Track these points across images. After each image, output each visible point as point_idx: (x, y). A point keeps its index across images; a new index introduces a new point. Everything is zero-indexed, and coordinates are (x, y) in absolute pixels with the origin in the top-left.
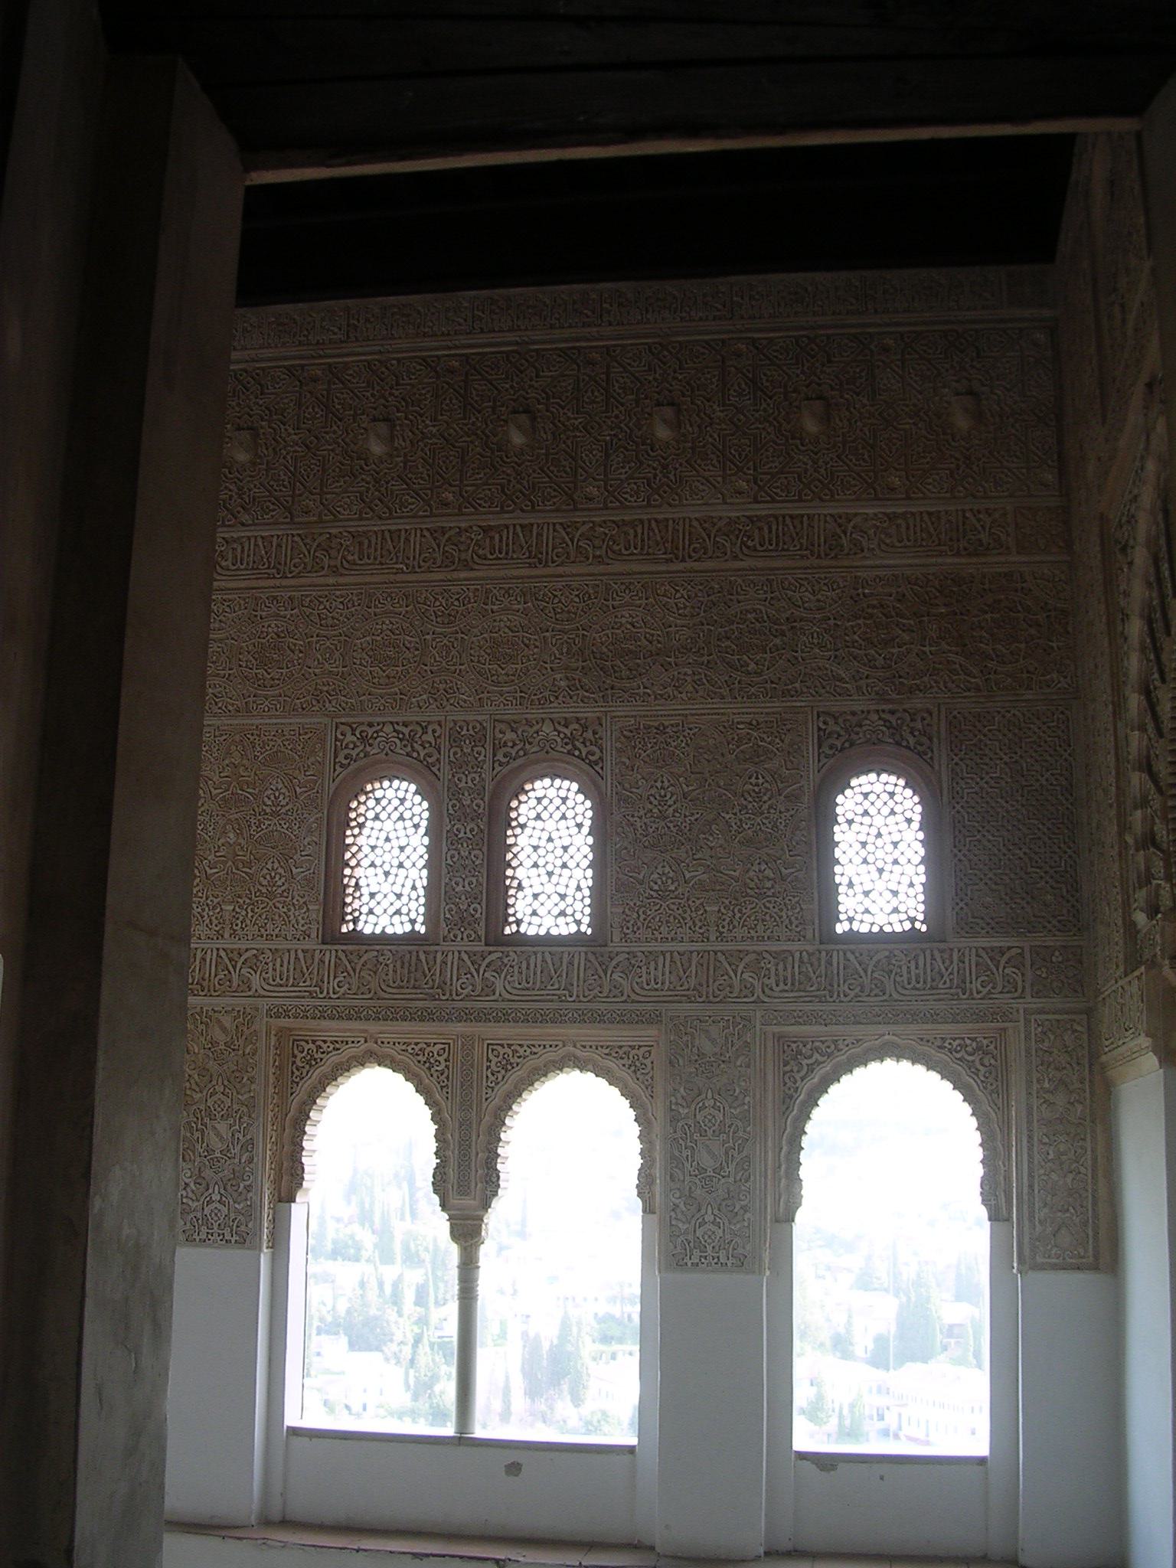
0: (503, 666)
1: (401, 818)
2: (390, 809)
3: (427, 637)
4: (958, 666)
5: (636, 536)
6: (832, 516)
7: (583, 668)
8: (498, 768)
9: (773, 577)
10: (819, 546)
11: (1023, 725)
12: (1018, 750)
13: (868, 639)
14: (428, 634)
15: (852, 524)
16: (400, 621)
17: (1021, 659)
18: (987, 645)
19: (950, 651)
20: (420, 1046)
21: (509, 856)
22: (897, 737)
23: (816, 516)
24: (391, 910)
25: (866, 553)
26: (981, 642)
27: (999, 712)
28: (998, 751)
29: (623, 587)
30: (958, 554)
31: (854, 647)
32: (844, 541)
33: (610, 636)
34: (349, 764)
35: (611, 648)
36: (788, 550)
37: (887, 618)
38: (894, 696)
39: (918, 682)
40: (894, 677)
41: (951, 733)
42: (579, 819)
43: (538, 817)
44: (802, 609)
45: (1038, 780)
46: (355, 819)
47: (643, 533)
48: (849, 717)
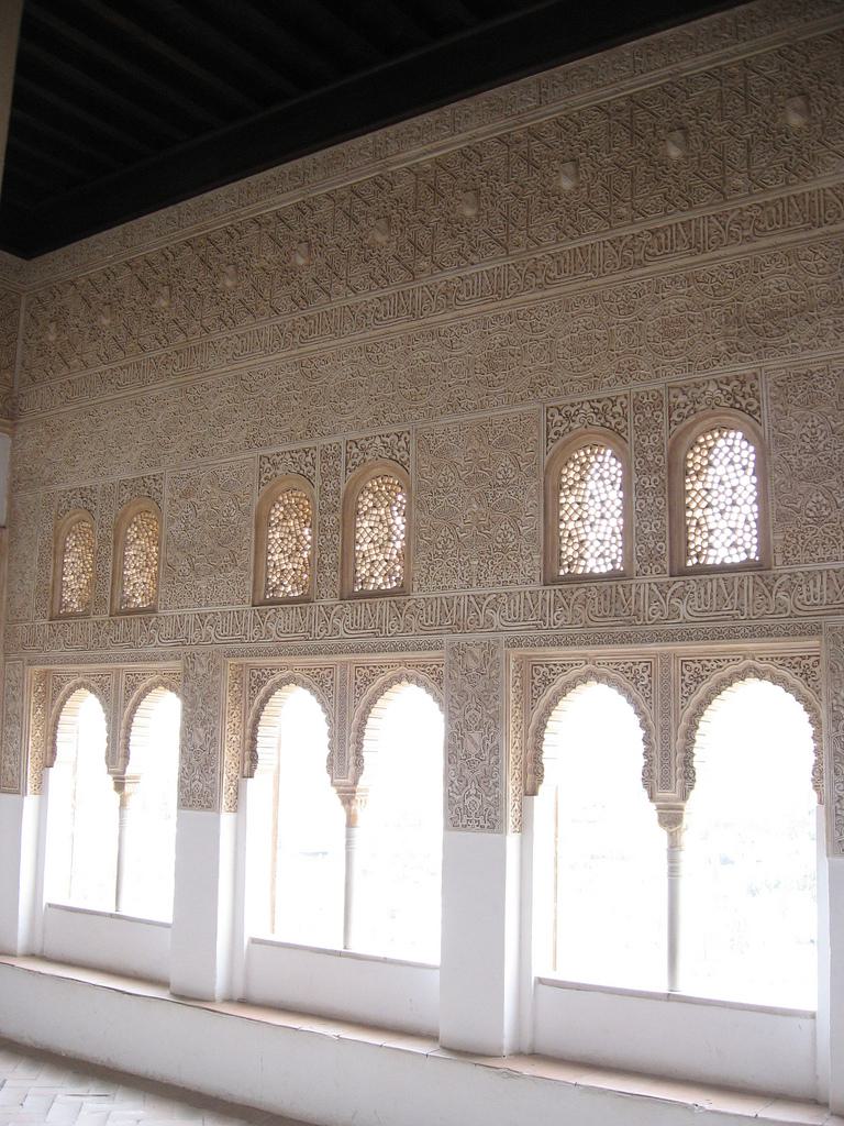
1: (731, 462)
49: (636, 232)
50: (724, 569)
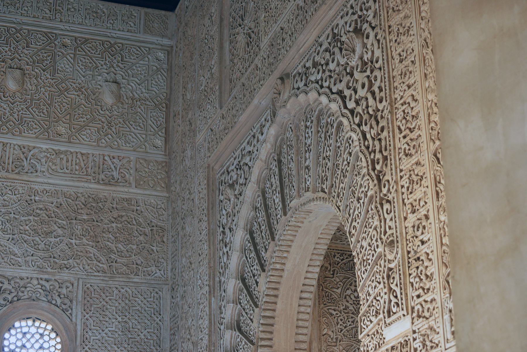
4: (92, 255)
10: (8, 164)
11: (131, 298)
12: (127, 314)
13: (35, 230)
15: (32, 153)
17: (133, 256)
18: (113, 244)
19: (88, 245)
22: (49, 298)
23: (9, 145)
25: (38, 174)
26: (108, 241)
27: (117, 288)
28: (114, 313)
30: (98, 183)
32: (25, 163)
38: (49, 270)
39: (66, 262)
40: (51, 257)
41: (85, 299)
45: (138, 335)
48: (18, 281)
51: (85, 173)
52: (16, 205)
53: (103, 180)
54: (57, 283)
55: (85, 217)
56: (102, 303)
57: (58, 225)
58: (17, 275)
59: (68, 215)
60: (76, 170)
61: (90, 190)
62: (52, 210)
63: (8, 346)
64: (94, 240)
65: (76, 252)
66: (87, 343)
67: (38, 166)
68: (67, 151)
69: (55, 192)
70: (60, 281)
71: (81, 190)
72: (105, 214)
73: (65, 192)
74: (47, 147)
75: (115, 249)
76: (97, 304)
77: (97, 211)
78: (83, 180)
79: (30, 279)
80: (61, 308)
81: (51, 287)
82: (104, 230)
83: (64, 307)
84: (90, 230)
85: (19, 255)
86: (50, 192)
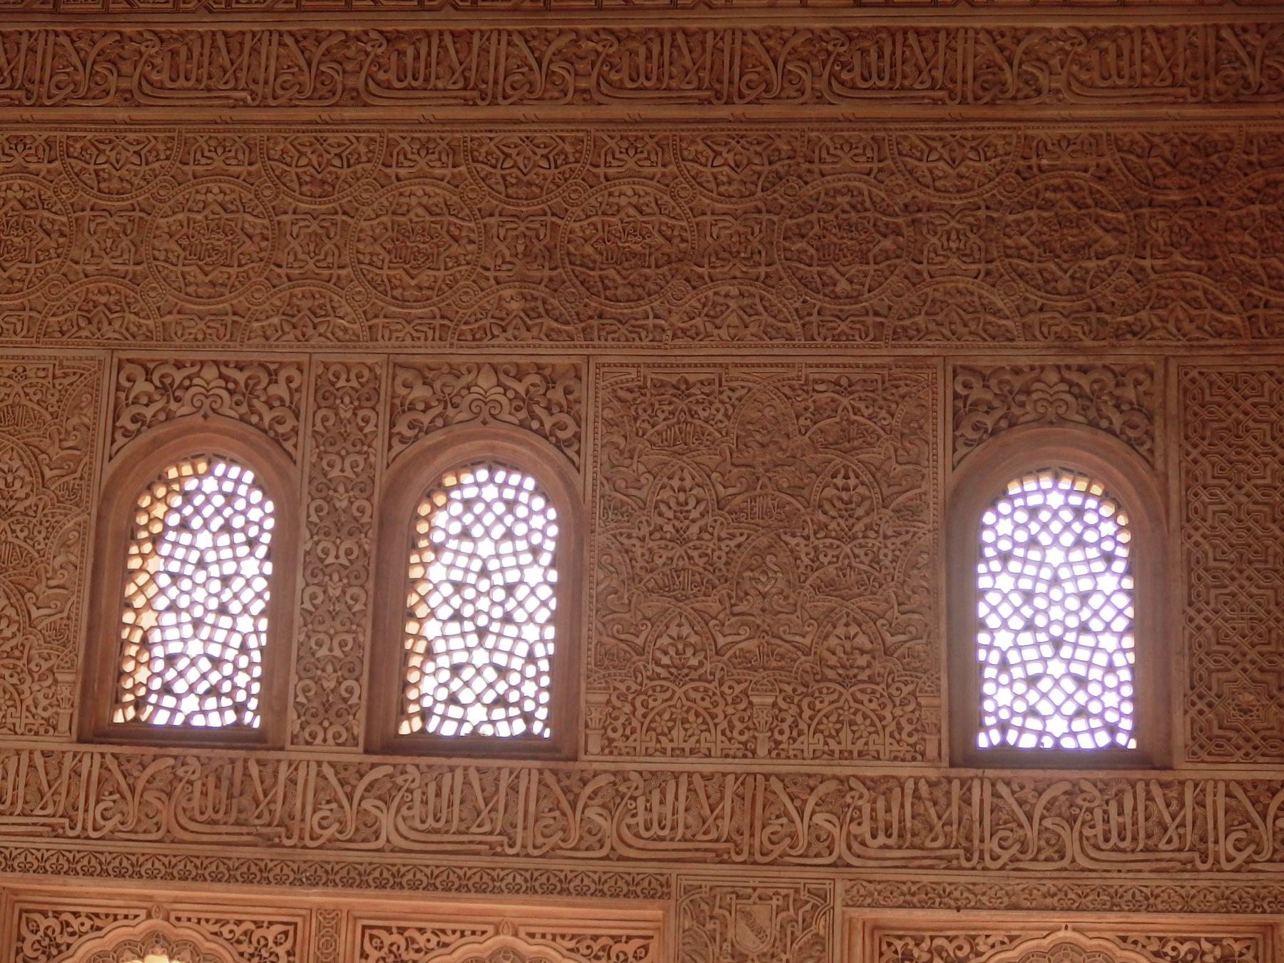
0: (414, 272)
1: (227, 528)
2: (208, 511)
3: (284, 218)
4: (1200, 294)
5: (649, 57)
6: (989, 32)
7: (551, 280)
8: (398, 447)
9: (882, 134)
10: (965, 82)
13: (1043, 243)
14: (286, 213)
15: (1023, 46)
16: (237, 189)
18: (1254, 258)
19: (1188, 268)
20: (244, 927)
21: (413, 599)
22: (1092, 414)
23: (961, 34)
24: (203, 687)
25: (1044, 98)
26: (1242, 253)
27: (1271, 374)
28: (1269, 441)
29: (625, 144)
30: (1207, 102)
31: (1020, 257)
33: (600, 227)
34: (139, 431)
35: (600, 246)
36: (911, 89)
37: (1079, 208)
38: (1088, 342)
39: (1129, 319)
41: (1186, 408)
42: (536, 539)
43: (465, 534)
44: (931, 191)
46: (146, 527)
47: (661, 54)
48: (1008, 377)
49: (352, 29)
50: (238, 739)
51: (1169, 81)
52: (990, 185)
53: (1218, 93)
54: (1111, 375)
55: (1176, 196)
56: (1234, 416)
57: (1104, 224)
58: (1003, 364)
59: (1127, 196)
60: (1144, 76)
61: (1186, 123)
62: (1086, 188)
63: (994, 545)
64: (1204, 253)
65: (1155, 291)
66: (1198, 523)
67: (1041, 78)
68: (1117, 29)
69: (1092, 140)
70: (1117, 369)
71: (1159, 128)
72: (1229, 183)
73: (1119, 136)
74: (1064, 25)
75: (1261, 272)
76: (1220, 420)
77: (1207, 177)
78: (1165, 99)
79: (1037, 372)
80: (1124, 437)
81: (1096, 387)
82: (1230, 225)
83: (1132, 434)
84: (1190, 230)
85: (1008, 313)
86: (1078, 141)
